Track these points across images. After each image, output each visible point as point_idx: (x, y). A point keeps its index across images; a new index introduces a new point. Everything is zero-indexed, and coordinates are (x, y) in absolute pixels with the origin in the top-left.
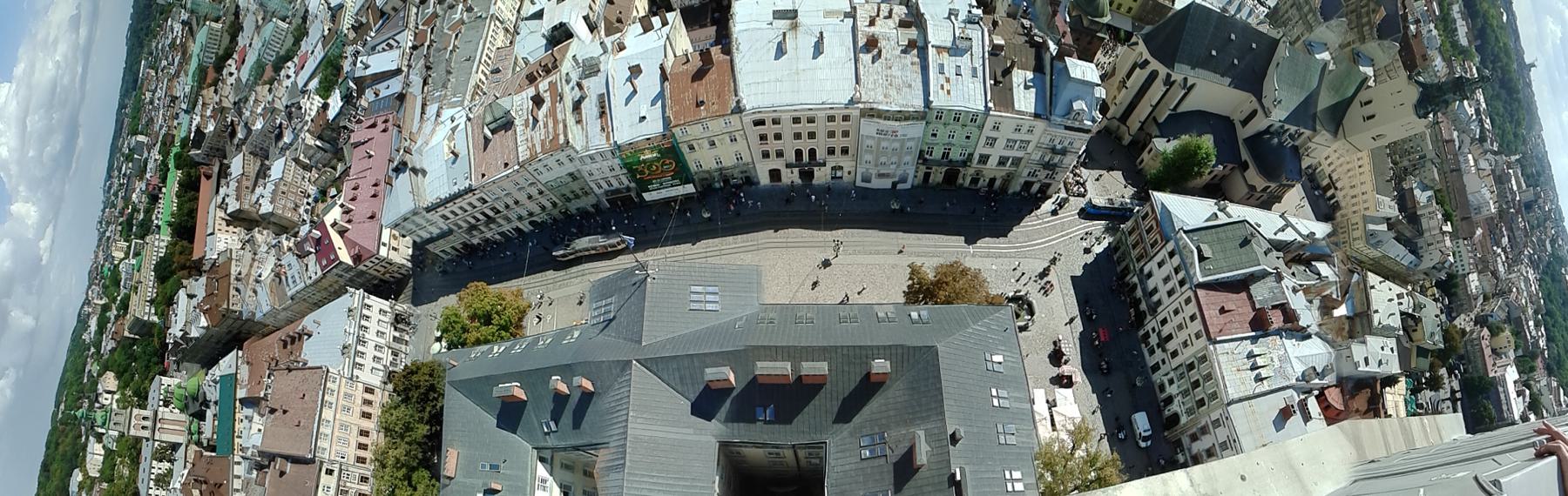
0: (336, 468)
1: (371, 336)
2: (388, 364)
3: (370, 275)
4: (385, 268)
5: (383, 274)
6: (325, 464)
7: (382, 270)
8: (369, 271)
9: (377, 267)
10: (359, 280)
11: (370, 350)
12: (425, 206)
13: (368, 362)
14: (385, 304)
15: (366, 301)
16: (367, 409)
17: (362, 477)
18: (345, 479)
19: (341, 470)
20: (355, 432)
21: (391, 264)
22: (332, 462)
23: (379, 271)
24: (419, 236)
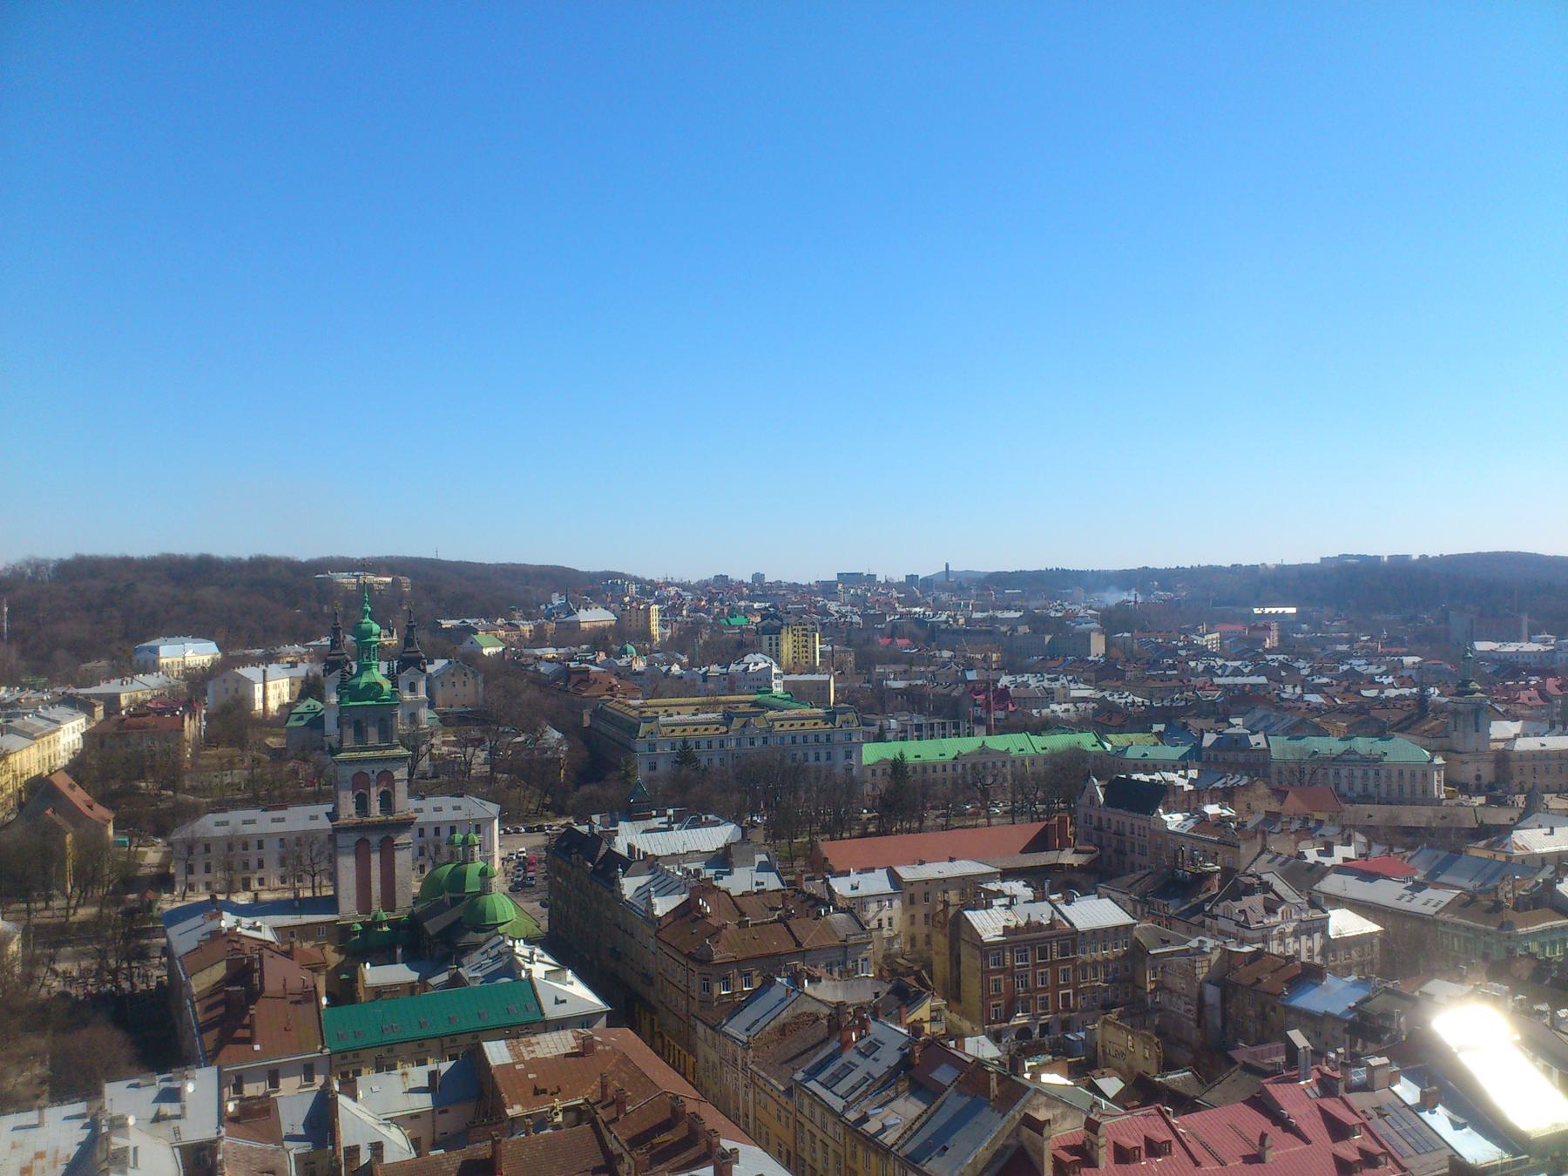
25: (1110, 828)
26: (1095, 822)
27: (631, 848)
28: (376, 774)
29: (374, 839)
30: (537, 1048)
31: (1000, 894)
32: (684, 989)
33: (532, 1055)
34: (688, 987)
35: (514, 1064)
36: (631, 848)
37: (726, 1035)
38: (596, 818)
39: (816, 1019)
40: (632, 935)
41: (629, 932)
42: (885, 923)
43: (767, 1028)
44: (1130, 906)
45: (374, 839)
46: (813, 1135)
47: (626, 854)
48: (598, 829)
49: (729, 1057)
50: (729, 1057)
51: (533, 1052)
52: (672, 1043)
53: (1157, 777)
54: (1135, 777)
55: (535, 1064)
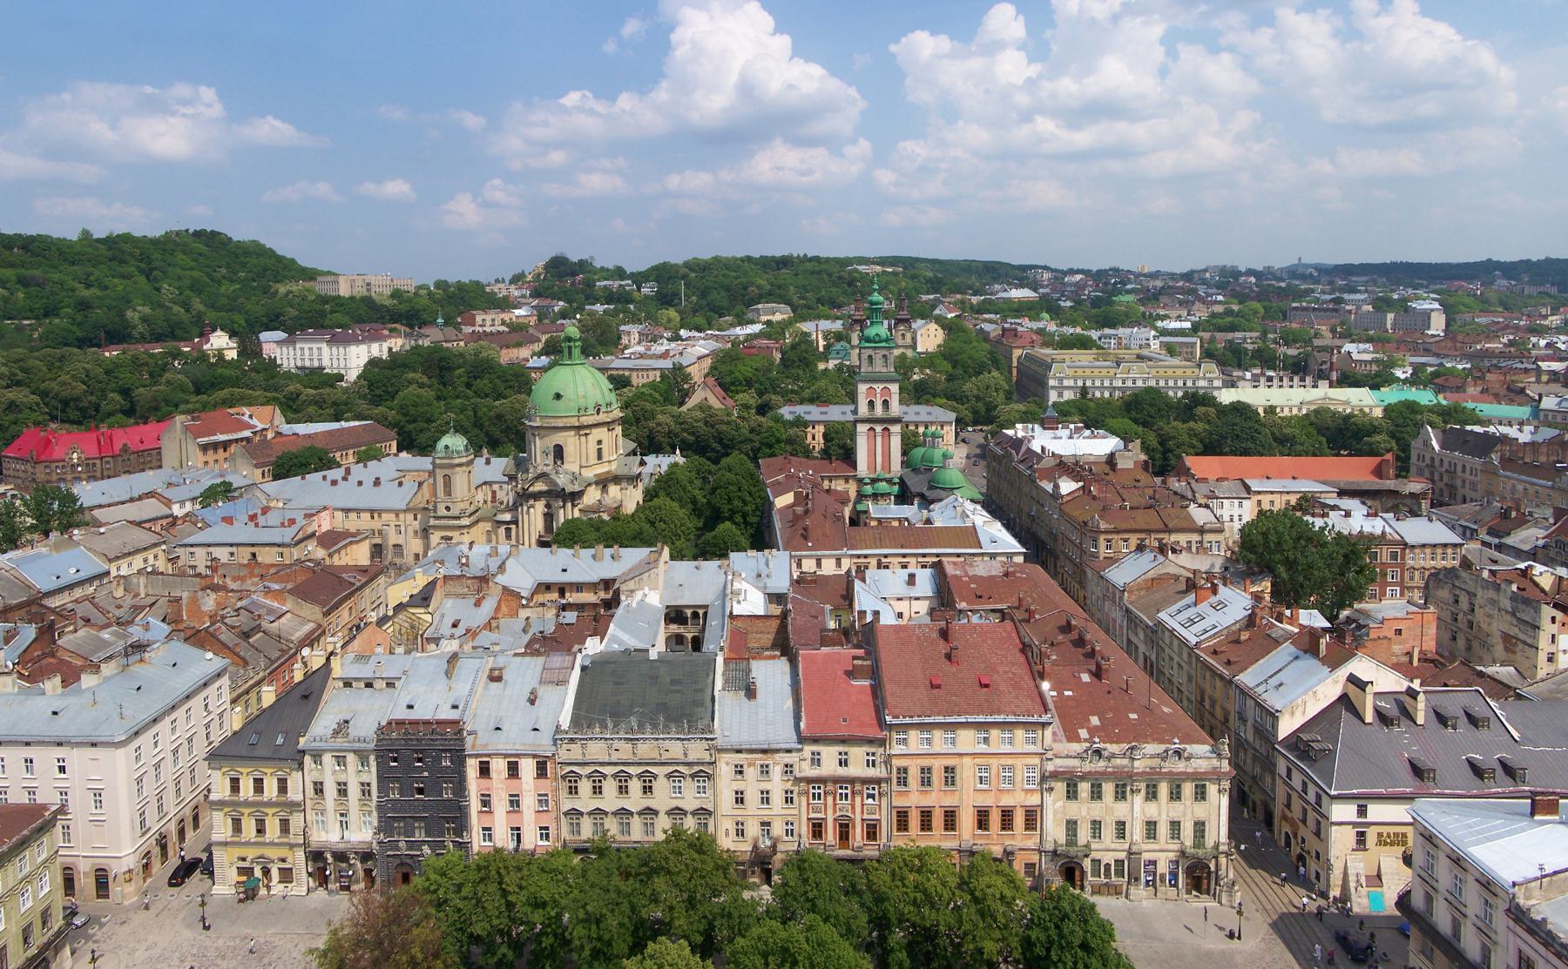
1: (1137, 809)
2: (1094, 855)
3: (1273, 790)
4: (1304, 821)
5: (1285, 817)
6: (881, 750)
7: (1296, 813)
8: (1278, 781)
9: (1297, 804)
10: (1249, 761)
11: (1109, 809)
12: (1521, 901)
13: (1084, 810)
14: (1218, 831)
15: (1212, 789)
16: (995, 819)
17: (875, 826)
18: (866, 791)
19: (878, 781)
20: (949, 801)
21: (1318, 834)
22: (888, 761)
23: (1288, 806)
24: (1429, 899)
25: (1441, 465)
26: (1428, 461)
27: (1043, 449)
31: (1335, 508)
36: (1043, 449)
38: (1019, 426)
39: (1177, 578)
42: (1236, 518)
44: (1460, 530)
46: (1171, 659)
48: (1020, 434)
53: (1491, 429)
54: (1468, 428)
55: (975, 579)
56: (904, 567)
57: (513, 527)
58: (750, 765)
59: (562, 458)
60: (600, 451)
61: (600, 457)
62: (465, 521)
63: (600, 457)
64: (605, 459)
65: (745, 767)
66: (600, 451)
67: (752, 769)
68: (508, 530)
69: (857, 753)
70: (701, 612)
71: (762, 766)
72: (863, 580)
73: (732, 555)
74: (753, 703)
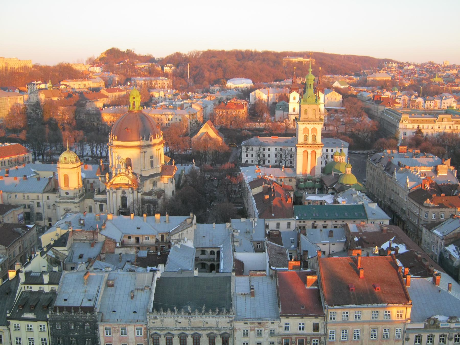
0: (321, 331)
27: (399, 164)
28: (311, 128)
29: (309, 151)
30: (366, 228)
32: (418, 216)
33: (365, 231)
34: (419, 215)
35: (358, 232)
36: (399, 164)
37: (434, 234)
40: (398, 194)
41: (397, 193)
43: (451, 233)
45: (309, 151)
47: (397, 164)
49: (435, 242)
50: (435, 242)
51: (365, 229)
52: (411, 234)
56: (325, 227)
57: (104, 204)
58: (251, 330)
59: (131, 166)
60: (152, 162)
61: (152, 166)
62: (77, 200)
63: (152, 166)
64: (154, 166)
65: (249, 331)
66: (152, 162)
67: (252, 332)
68: (101, 206)
69: (309, 322)
70: (216, 251)
71: (258, 330)
72: (305, 234)
73: (233, 220)
74: (253, 298)
